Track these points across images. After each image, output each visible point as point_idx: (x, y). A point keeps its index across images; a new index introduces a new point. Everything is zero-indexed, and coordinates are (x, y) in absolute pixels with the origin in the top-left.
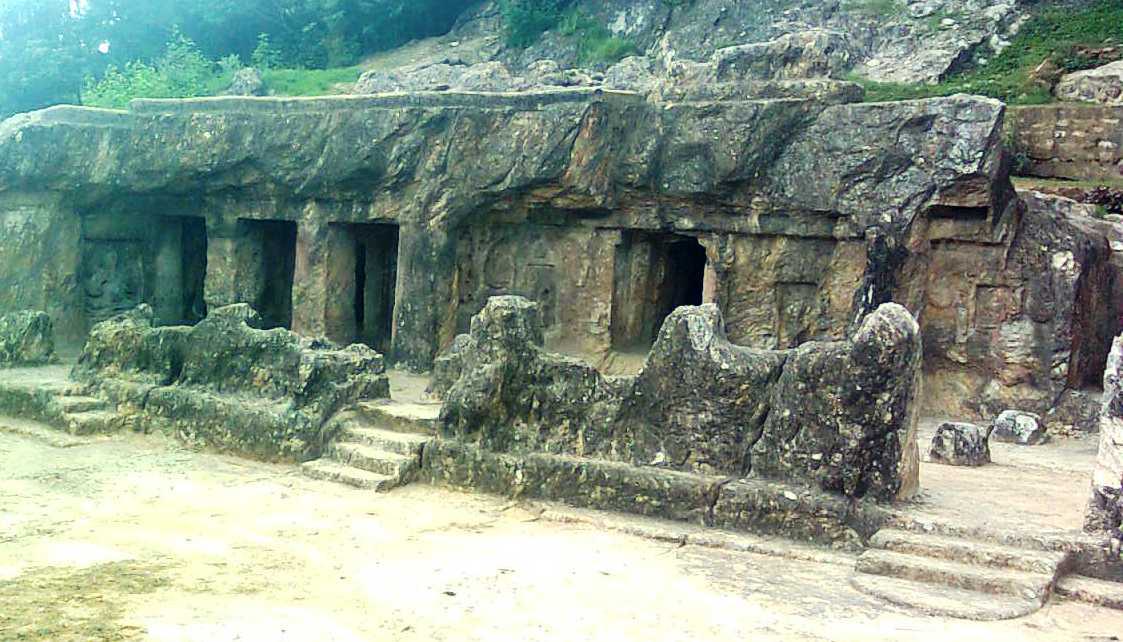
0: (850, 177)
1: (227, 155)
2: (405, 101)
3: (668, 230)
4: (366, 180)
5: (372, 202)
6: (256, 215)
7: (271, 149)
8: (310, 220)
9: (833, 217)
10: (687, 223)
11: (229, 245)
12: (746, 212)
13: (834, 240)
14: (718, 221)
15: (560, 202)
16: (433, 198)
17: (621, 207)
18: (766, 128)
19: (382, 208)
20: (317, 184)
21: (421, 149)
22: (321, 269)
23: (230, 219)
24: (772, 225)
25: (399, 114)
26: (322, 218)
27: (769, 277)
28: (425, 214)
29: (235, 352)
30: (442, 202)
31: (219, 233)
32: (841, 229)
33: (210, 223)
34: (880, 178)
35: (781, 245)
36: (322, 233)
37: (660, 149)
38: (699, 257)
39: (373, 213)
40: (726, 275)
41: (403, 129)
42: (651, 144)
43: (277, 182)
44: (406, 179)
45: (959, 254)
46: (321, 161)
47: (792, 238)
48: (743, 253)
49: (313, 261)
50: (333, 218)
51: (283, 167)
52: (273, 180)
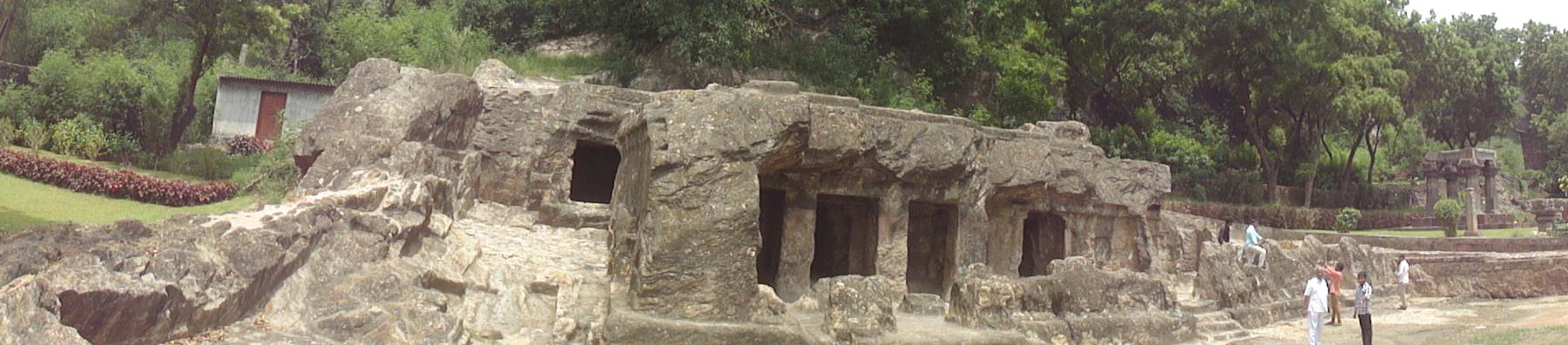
0: (1123, 191)
5: (949, 188)
6: (841, 191)
8: (893, 201)
9: (1119, 207)
19: (952, 194)
23: (813, 194)
26: (906, 197)
28: (977, 199)
31: (802, 202)
32: (1121, 214)
33: (791, 195)
36: (903, 207)
38: (1063, 224)
40: (1075, 234)
43: (883, 170)
47: (1100, 217)
48: (1081, 225)
49: (893, 229)
50: (915, 197)
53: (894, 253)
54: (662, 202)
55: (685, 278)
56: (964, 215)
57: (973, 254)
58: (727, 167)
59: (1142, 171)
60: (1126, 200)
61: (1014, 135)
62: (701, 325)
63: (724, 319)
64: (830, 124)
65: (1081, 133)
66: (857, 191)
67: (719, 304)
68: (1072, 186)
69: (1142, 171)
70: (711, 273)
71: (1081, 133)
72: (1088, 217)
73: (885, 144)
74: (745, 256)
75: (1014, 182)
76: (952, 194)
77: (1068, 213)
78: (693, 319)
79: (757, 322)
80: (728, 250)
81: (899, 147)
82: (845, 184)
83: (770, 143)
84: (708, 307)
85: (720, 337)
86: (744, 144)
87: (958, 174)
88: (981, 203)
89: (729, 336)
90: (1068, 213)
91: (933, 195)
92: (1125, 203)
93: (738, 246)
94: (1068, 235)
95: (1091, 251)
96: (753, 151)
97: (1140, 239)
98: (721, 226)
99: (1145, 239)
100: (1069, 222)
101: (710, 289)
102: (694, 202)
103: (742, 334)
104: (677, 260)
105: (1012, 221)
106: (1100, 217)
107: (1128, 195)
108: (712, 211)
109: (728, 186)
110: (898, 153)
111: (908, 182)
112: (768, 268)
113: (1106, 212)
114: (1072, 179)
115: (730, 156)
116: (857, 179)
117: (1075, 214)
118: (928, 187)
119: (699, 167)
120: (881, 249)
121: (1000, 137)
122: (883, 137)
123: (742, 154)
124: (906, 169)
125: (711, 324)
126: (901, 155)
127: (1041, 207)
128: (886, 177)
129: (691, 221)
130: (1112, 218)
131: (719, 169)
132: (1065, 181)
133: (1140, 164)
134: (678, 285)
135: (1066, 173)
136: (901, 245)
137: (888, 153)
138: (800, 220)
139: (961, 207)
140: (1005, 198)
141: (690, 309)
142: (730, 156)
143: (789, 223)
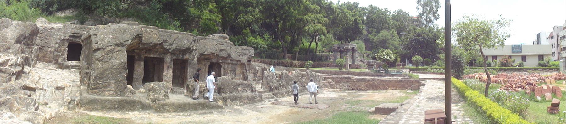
0: (239, 56)
6: (152, 56)
8: (168, 59)
9: (238, 61)
19: (186, 57)
20: (174, 50)
28: (194, 58)
32: (239, 63)
38: (221, 66)
40: (224, 69)
48: (226, 66)
49: (168, 67)
50: (175, 58)
53: (168, 75)
54: (97, 60)
55: (105, 84)
56: (190, 63)
58: (117, 48)
59: (245, 49)
60: (240, 58)
61: (206, 38)
62: (110, 98)
63: (117, 96)
64: (148, 35)
65: (226, 38)
67: (115, 92)
68: (224, 54)
69: (245, 49)
70: (112, 82)
71: (226, 38)
72: (229, 64)
73: (166, 41)
74: (123, 76)
75: (206, 53)
76: (186, 57)
77: (222, 63)
78: (107, 96)
79: (127, 96)
80: (118, 74)
82: (153, 53)
83: (130, 41)
84: (112, 92)
85: (116, 101)
86: (122, 41)
87: (188, 50)
88: (195, 60)
89: (119, 101)
90: (222, 63)
91: (180, 57)
93: (121, 73)
94: (222, 69)
96: (125, 44)
97: (244, 71)
98: (115, 67)
99: (246, 71)
100: (223, 65)
101: (112, 87)
102: (107, 60)
103: (122, 101)
104: (102, 78)
105: (205, 65)
107: (241, 57)
108: (112, 63)
109: (117, 55)
111: (172, 54)
112: (130, 80)
113: (234, 62)
115: (117, 45)
116: (157, 52)
118: (179, 54)
119: (108, 49)
120: (164, 74)
121: (201, 39)
123: (121, 45)
124: (172, 49)
125: (113, 98)
126: (171, 45)
127: (214, 61)
128: (166, 51)
129: (106, 66)
130: (236, 64)
131: (114, 49)
132: (221, 53)
133: (245, 47)
134: (102, 86)
135: (221, 50)
136: (171, 73)
137: (167, 44)
139: (189, 61)
140: (203, 58)
141: (107, 93)
142: (117, 45)
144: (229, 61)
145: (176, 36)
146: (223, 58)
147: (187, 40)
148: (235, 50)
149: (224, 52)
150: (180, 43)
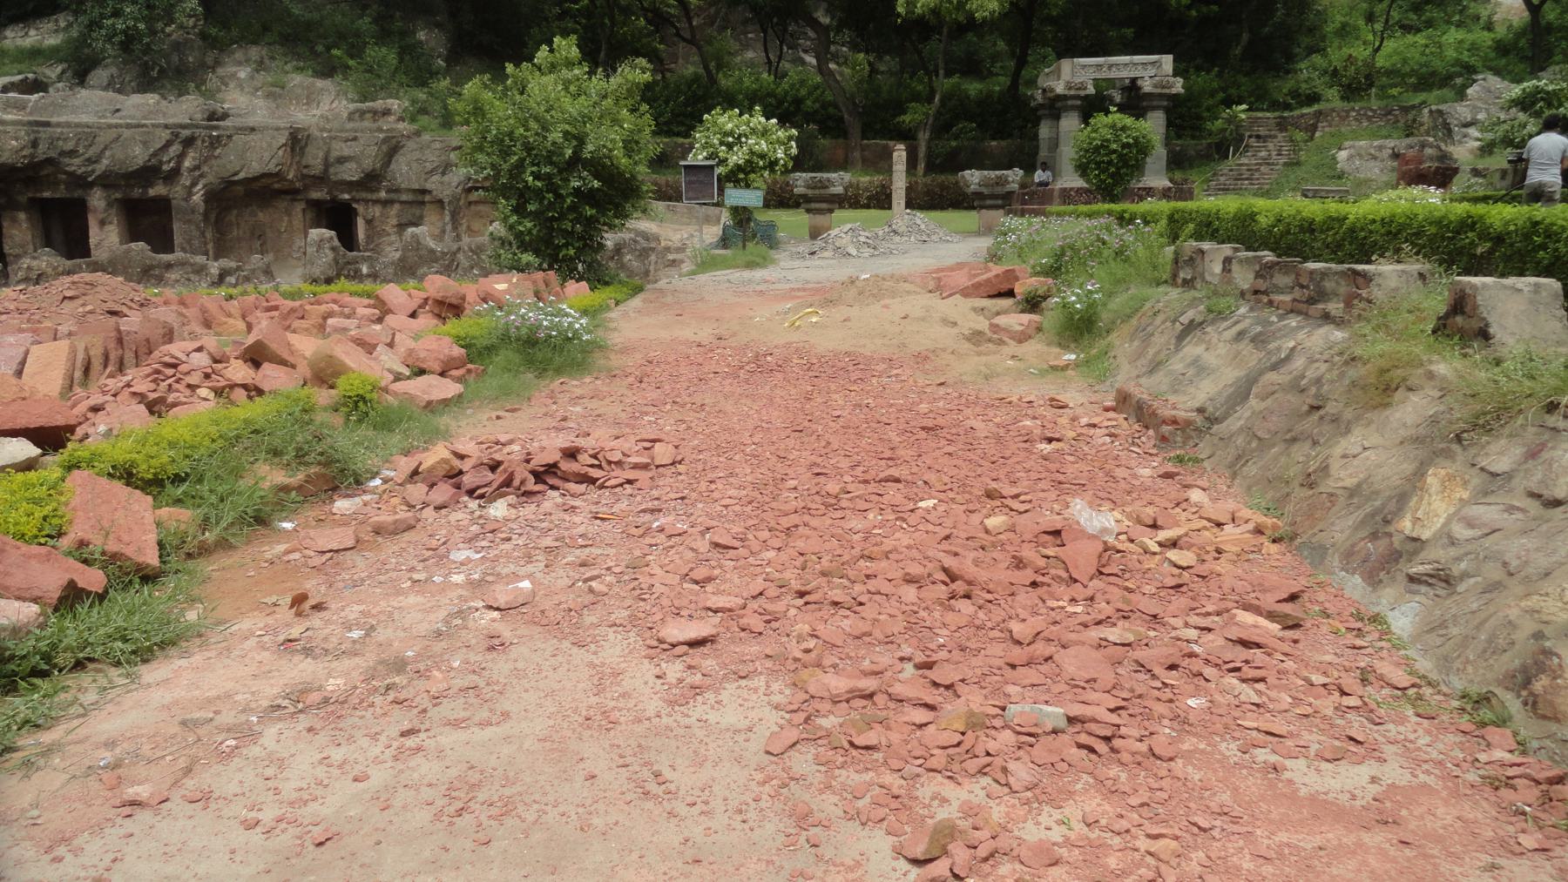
0: (432, 172)
1: (32, 156)
2: (166, 127)
3: (334, 200)
4: (149, 173)
5: (151, 185)
6: (46, 194)
7: (63, 153)
8: (97, 200)
9: (424, 192)
10: (347, 196)
11: (22, 216)
12: (378, 190)
13: (423, 203)
14: (364, 195)
15: (276, 186)
16: (194, 184)
17: (306, 188)
18: (385, 148)
21: (181, 157)
22: (109, 228)
23: (23, 199)
24: (393, 196)
25: (165, 135)
27: (394, 221)
28: (190, 194)
29: (151, 267)
30: (199, 187)
31: (13, 206)
32: (427, 198)
34: (443, 174)
35: (397, 206)
36: (110, 205)
37: (326, 159)
38: (355, 213)
39: (152, 192)
40: (369, 222)
41: (169, 144)
42: (321, 154)
43: (71, 174)
44: (175, 173)
45: (481, 208)
46: (105, 162)
47: (402, 202)
48: (376, 211)
49: (102, 223)
50: (118, 195)
51: (74, 165)
52: (66, 173)
53: (106, 243)
57: (189, 242)
65: (387, 112)
66: (61, 193)
68: (350, 172)
71: (387, 112)
72: (386, 203)
73: (72, 153)
75: (242, 175)
81: (91, 153)
88: (197, 198)
90: (357, 201)
91: (137, 193)
92: (428, 186)
94: (360, 223)
95: (393, 238)
100: (360, 208)
106: (402, 202)
107: (436, 178)
110: (88, 160)
111: (108, 181)
113: (404, 197)
114: (348, 165)
116: (57, 183)
117: (367, 201)
122: (69, 146)
126: (90, 161)
128: (82, 182)
130: (423, 203)
135: (341, 160)
137: (76, 161)
138: (14, 220)
143: (5, 224)
144: (383, 194)
145: (113, 133)
146: (350, 186)
147: (145, 143)
148: (417, 155)
149: (353, 165)
150: (120, 155)
